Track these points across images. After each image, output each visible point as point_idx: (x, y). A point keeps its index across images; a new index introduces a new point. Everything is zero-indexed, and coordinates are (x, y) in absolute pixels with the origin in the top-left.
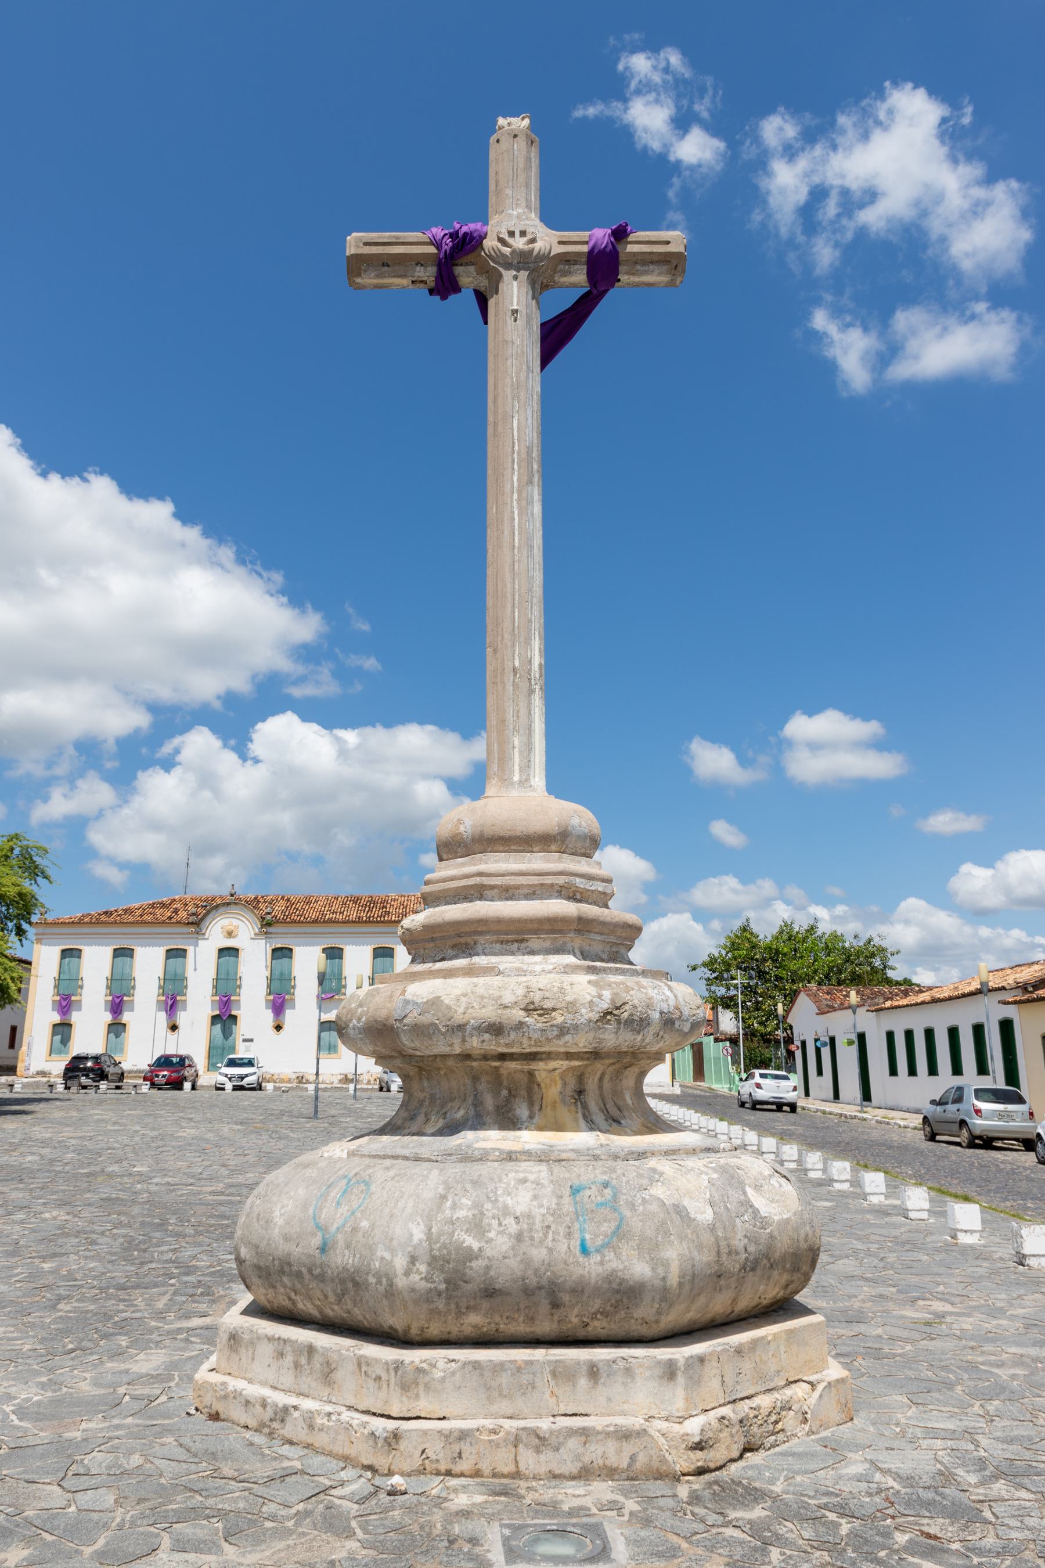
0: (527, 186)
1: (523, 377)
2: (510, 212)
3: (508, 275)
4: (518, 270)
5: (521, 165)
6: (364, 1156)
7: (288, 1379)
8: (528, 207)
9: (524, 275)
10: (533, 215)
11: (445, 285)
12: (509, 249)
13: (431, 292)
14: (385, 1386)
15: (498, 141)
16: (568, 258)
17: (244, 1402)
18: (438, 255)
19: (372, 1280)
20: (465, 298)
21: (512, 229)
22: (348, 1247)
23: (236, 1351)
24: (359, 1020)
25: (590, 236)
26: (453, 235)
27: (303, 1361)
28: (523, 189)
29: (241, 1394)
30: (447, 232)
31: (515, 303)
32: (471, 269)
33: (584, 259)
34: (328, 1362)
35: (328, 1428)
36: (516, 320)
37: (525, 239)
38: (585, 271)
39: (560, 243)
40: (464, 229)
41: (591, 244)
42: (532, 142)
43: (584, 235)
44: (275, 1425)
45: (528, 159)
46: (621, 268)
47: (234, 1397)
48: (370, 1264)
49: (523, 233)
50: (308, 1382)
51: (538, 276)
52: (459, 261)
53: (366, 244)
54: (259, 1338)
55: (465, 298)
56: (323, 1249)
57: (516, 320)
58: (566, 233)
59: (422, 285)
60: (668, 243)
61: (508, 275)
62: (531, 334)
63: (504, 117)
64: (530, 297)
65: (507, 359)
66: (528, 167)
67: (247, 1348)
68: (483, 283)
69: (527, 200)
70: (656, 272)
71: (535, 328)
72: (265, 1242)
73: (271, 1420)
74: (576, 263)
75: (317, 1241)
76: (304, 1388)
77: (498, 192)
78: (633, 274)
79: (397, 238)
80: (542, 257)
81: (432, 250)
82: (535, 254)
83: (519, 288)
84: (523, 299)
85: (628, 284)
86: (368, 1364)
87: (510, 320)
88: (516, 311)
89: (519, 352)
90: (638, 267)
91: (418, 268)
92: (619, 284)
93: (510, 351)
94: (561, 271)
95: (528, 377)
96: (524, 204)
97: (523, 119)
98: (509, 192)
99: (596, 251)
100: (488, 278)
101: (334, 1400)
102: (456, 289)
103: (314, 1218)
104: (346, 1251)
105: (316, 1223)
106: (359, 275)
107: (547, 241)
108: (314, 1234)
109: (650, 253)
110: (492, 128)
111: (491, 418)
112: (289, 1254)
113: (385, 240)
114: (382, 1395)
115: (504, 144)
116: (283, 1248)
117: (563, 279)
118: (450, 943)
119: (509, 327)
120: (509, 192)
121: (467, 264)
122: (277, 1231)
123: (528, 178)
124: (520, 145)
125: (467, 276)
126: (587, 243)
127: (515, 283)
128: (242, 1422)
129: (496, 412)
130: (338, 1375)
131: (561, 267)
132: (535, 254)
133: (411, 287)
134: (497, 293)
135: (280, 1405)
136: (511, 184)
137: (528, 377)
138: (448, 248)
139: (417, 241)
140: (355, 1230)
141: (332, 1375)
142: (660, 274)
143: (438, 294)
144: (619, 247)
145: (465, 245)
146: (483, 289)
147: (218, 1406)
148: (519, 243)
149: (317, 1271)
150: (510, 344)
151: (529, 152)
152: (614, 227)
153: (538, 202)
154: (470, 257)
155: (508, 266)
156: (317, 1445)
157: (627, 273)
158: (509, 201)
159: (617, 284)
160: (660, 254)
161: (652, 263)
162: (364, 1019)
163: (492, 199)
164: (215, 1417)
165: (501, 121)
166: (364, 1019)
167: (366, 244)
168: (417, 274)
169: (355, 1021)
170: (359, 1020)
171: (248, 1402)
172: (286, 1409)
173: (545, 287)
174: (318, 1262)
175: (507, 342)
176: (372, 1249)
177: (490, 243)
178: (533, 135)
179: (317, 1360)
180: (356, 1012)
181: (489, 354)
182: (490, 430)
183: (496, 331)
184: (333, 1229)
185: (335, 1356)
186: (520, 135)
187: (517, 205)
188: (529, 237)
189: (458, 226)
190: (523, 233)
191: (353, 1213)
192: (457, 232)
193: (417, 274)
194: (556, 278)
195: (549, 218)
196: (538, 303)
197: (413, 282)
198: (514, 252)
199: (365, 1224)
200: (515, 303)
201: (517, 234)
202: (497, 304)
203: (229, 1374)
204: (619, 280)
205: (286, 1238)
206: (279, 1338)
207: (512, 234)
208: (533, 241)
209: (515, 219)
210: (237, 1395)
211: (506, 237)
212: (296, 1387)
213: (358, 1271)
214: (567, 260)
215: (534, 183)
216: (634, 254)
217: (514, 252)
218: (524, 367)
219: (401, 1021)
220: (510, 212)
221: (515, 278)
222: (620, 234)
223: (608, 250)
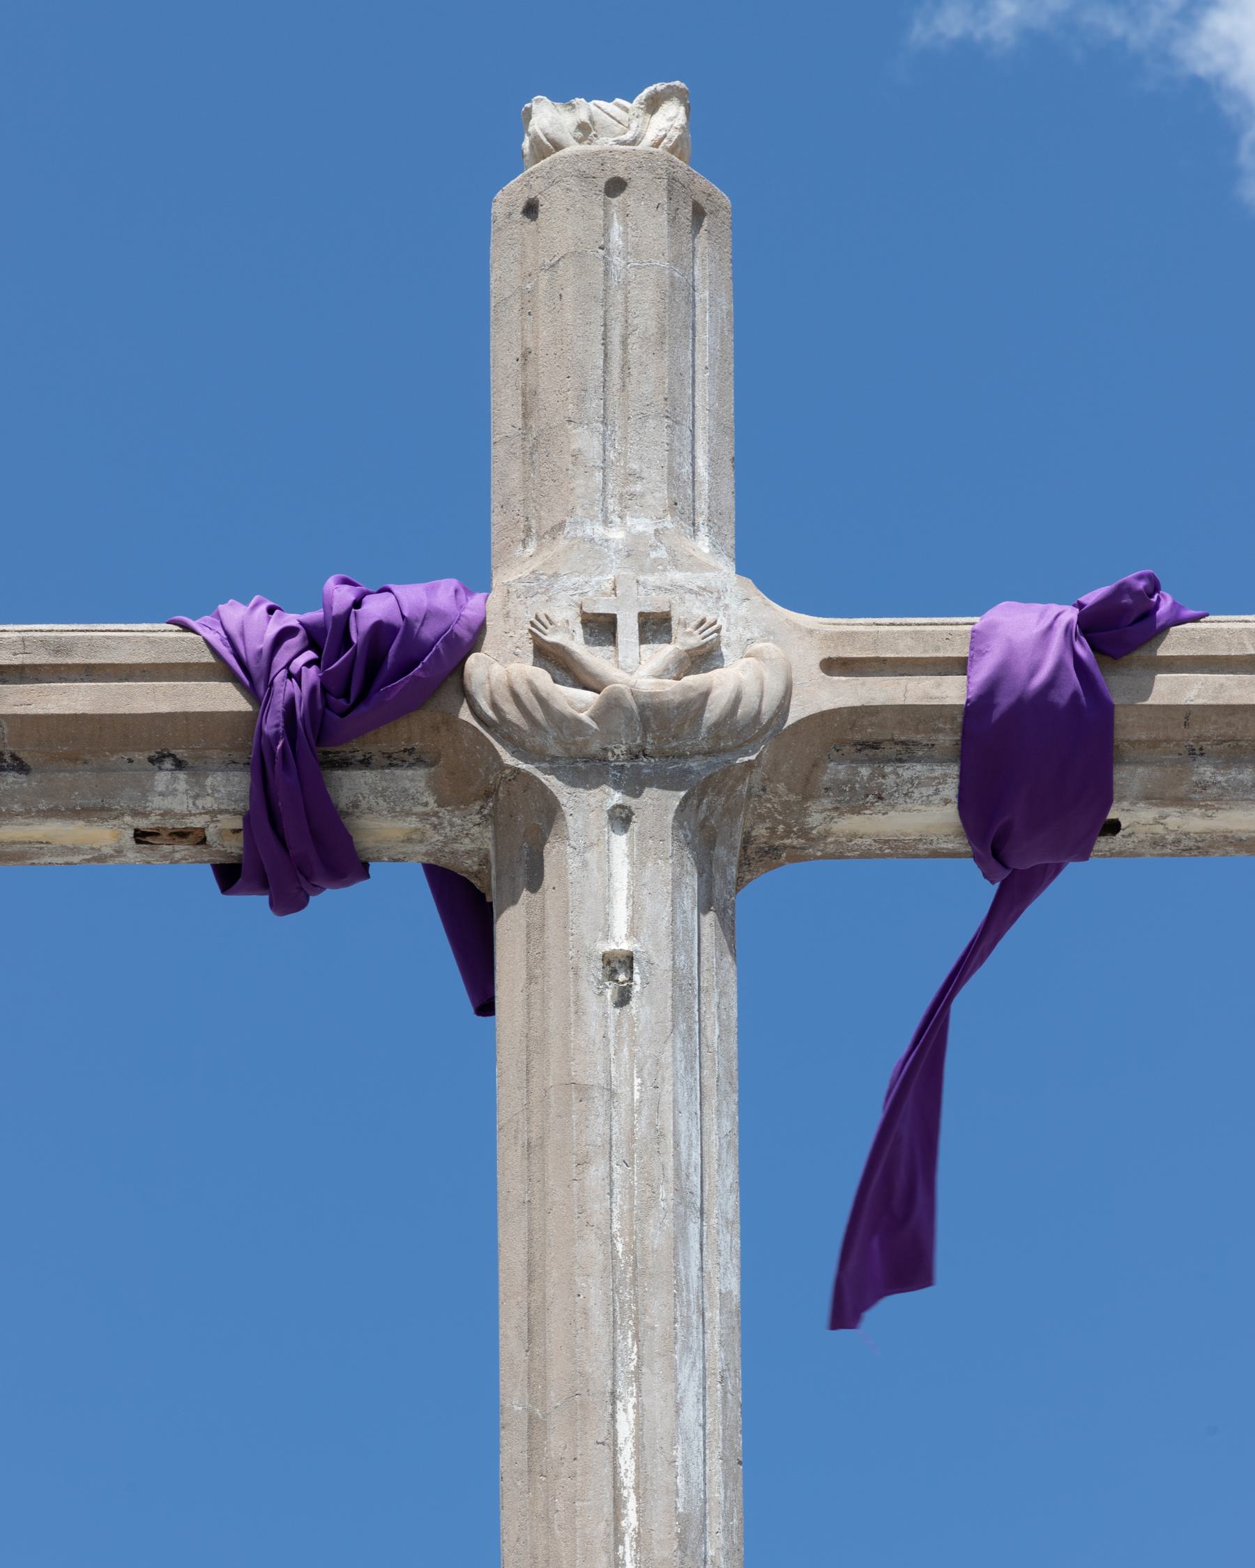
0: (676, 413)
1: (657, 1236)
2: (599, 530)
3: (584, 807)
4: (634, 786)
5: (646, 318)
8: (681, 507)
9: (660, 805)
10: (703, 545)
11: (291, 845)
12: (589, 696)
13: (229, 877)
15: (531, 209)
16: (871, 733)
18: (253, 722)
20: (386, 913)
21: (602, 608)
25: (977, 638)
26: (326, 637)
28: (656, 430)
30: (292, 620)
31: (620, 925)
32: (414, 780)
33: (948, 739)
36: (623, 999)
37: (662, 653)
38: (951, 790)
39: (833, 666)
40: (376, 609)
42: (699, 214)
43: (948, 633)
45: (680, 294)
46: (1122, 776)
49: (655, 626)
51: (730, 813)
52: (356, 748)
55: (386, 913)
57: (623, 999)
58: (860, 625)
59: (182, 850)
61: (584, 807)
62: (696, 1056)
63: (562, 96)
64: (689, 899)
65: (583, 1163)
66: (678, 326)
68: (468, 840)
69: (673, 477)
71: (713, 1033)
74: (906, 752)
77: (535, 445)
80: (740, 729)
81: (226, 698)
82: (712, 713)
83: (637, 864)
84: (659, 909)
85: (1157, 842)
87: (597, 1001)
88: (628, 961)
89: (641, 1129)
90: (1206, 771)
91: (162, 779)
92: (1117, 841)
93: (598, 1127)
94: (836, 788)
95: (680, 1236)
96: (659, 496)
97: (653, 105)
98: (586, 441)
99: (1004, 701)
100: (490, 818)
102: (345, 864)
107: (771, 657)
110: (506, 149)
111: (513, 1399)
115: (566, 219)
117: (848, 824)
119: (593, 1028)
120: (586, 441)
121: (391, 761)
123: (683, 378)
124: (640, 233)
125: (394, 811)
126: (960, 666)
127: (620, 843)
129: (536, 1379)
131: (837, 771)
132: (712, 713)
133: (134, 855)
134: (535, 880)
136: (595, 405)
137: (680, 1236)
138: (301, 693)
139: (151, 660)
143: (262, 884)
144: (1116, 687)
145: (381, 678)
146: (468, 865)
148: (637, 669)
150: (599, 1103)
151: (682, 259)
152: (1090, 598)
153: (728, 486)
154: (410, 730)
155: (587, 768)
157: (1149, 798)
158: (585, 485)
159: (1103, 844)
163: (507, 473)
165: (546, 117)
168: (157, 802)
173: (760, 856)
175: (583, 1091)
177: (497, 670)
178: (702, 183)
181: (503, 1141)
182: (512, 1449)
183: (534, 1045)
186: (638, 181)
187: (628, 500)
188: (684, 640)
189: (343, 596)
190: (655, 626)
192: (343, 622)
193: (157, 802)
194: (815, 820)
195: (775, 559)
196: (728, 925)
197: (140, 836)
198: (611, 707)
200: (620, 925)
201: (628, 628)
202: (535, 930)
204: (1114, 827)
207: (601, 628)
208: (704, 658)
209: (619, 565)
211: (576, 643)
214: (867, 741)
215: (710, 400)
216: (1188, 714)
217: (611, 707)
218: (665, 1194)
220: (599, 530)
221: (621, 819)
222: (1121, 627)
223: (1062, 697)
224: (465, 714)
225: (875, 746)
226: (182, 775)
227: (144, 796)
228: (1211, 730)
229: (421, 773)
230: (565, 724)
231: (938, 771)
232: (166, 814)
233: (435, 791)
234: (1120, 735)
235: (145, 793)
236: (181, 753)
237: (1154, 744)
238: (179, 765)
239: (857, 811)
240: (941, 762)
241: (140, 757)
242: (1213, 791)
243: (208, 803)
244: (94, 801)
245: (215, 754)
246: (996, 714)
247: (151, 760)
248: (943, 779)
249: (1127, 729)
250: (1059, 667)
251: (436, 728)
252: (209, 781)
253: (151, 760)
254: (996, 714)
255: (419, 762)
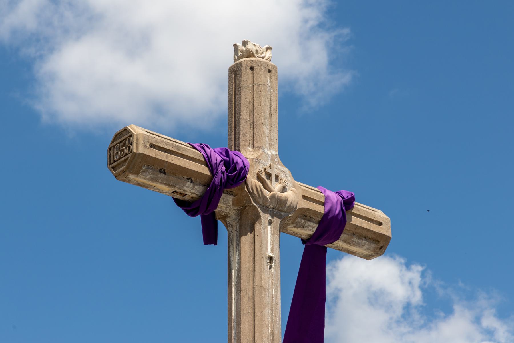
16: (307, 214)
32: (230, 198)
33: (319, 219)
41: (328, 207)
53: (152, 146)
60: (380, 224)
70: (365, 247)
78: (348, 243)
79: (178, 148)
90: (355, 239)
91: (188, 183)
94: (297, 223)
99: (331, 215)
106: (137, 173)
109: (368, 230)
113: (168, 147)
131: (299, 219)
142: (368, 249)
157: (344, 241)
160: (375, 233)
161: (365, 238)
167: (152, 146)
168: (185, 188)
216: (356, 227)
224: (246, 189)
225: (306, 216)
226: (192, 184)
227: (183, 186)
228: (359, 231)
229: (232, 197)
230: (264, 197)
231: (315, 225)
232: (185, 191)
233: (233, 201)
234: (345, 228)
235: (184, 185)
236: (193, 179)
237: (349, 230)
238: (192, 182)
239: (297, 228)
240: (316, 223)
241: (186, 177)
242: (354, 243)
243: (193, 191)
244: (174, 184)
245: (199, 181)
246: (329, 217)
247: (187, 179)
248: (314, 227)
249: (347, 227)
250: (340, 211)
251: (239, 190)
252: (196, 187)
253: (187, 179)
254: (329, 217)
255: (232, 195)
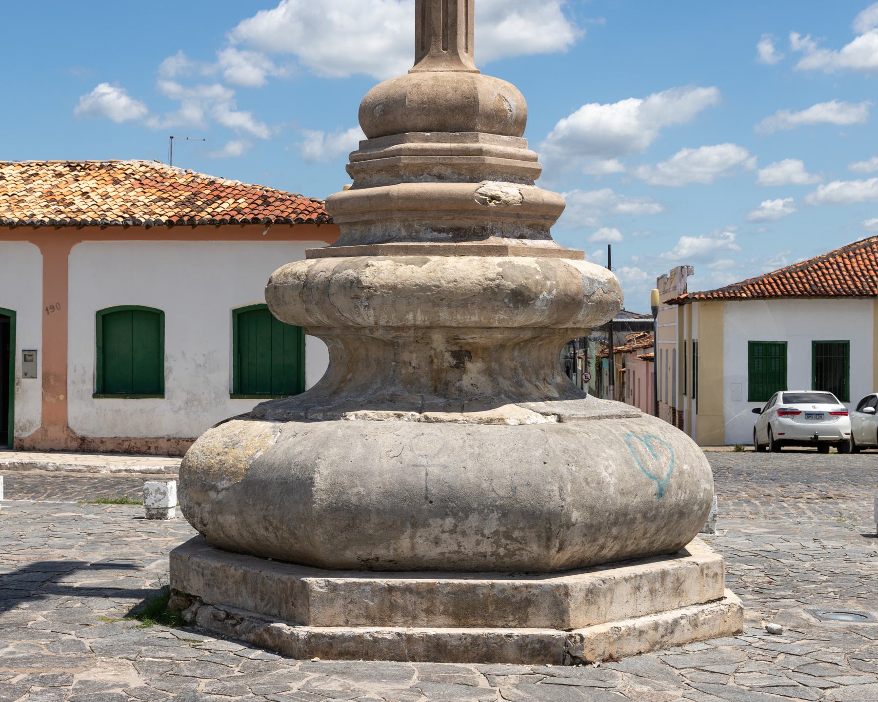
6: (581, 418)
7: (645, 606)
14: (720, 578)
17: (637, 633)
19: (696, 508)
22: (680, 487)
23: (595, 603)
24: (550, 292)
27: (657, 586)
29: (635, 629)
34: (678, 579)
35: (709, 619)
44: (666, 639)
47: (629, 634)
48: (696, 496)
50: (662, 600)
54: (617, 583)
56: (660, 494)
67: (605, 596)
72: (601, 502)
73: (663, 636)
75: (654, 488)
76: (659, 607)
86: (708, 568)
101: (683, 605)
103: (644, 471)
104: (680, 492)
105: (648, 475)
108: (649, 484)
112: (626, 506)
114: (718, 586)
116: (620, 501)
118: (530, 222)
122: (612, 489)
128: (636, 651)
130: (686, 586)
135: (670, 622)
140: (681, 473)
141: (681, 587)
147: (613, 650)
149: (654, 512)
156: (699, 637)
162: (554, 292)
164: (611, 658)
166: (554, 292)
169: (545, 293)
170: (550, 292)
171: (641, 632)
172: (676, 622)
174: (655, 506)
176: (697, 484)
179: (669, 580)
180: (545, 285)
184: (665, 475)
185: (683, 572)
191: (673, 461)
199: (685, 467)
203: (589, 625)
205: (623, 493)
206: (636, 576)
210: (630, 631)
212: (652, 608)
213: (686, 504)
219: (588, 297)
